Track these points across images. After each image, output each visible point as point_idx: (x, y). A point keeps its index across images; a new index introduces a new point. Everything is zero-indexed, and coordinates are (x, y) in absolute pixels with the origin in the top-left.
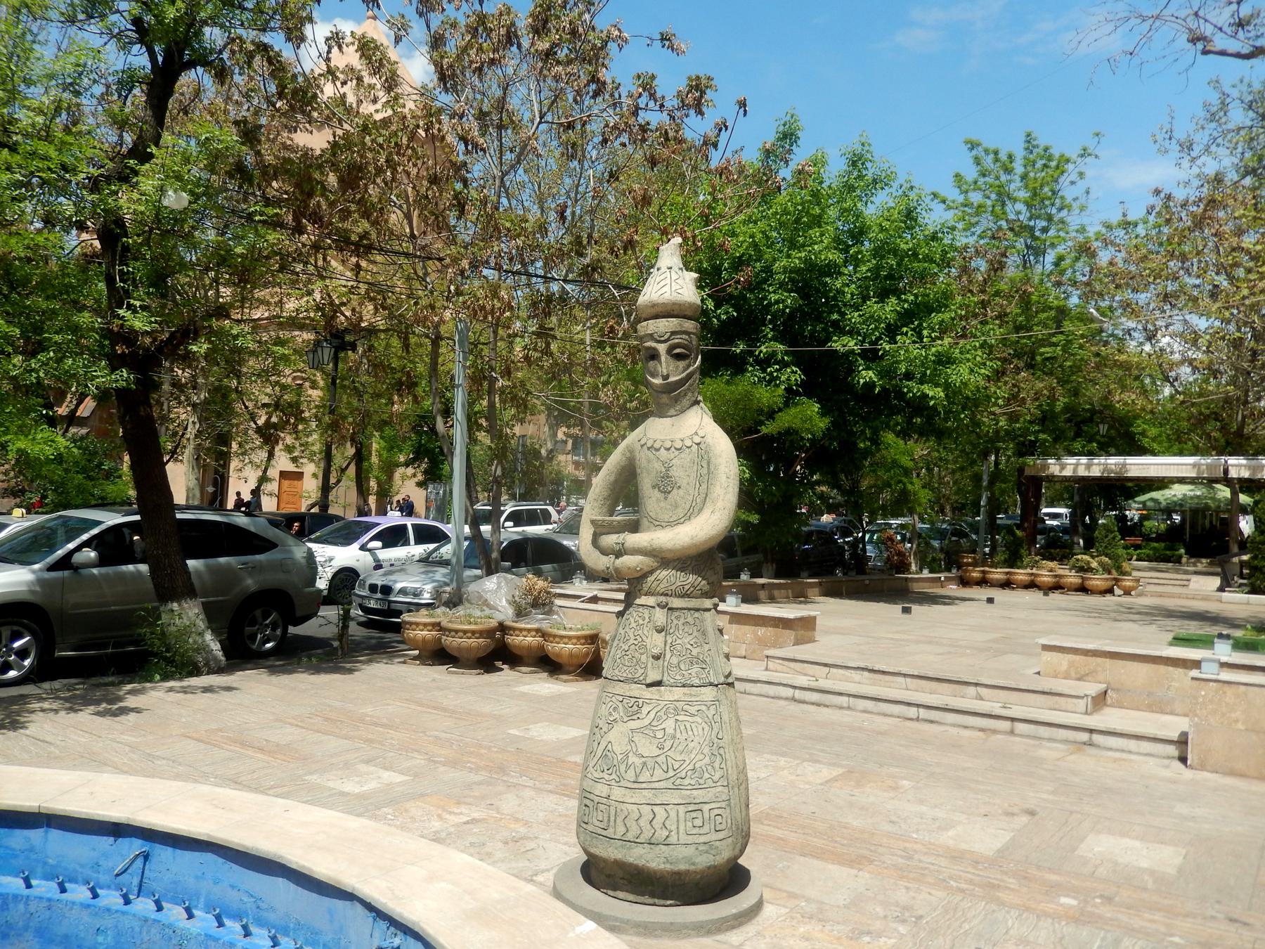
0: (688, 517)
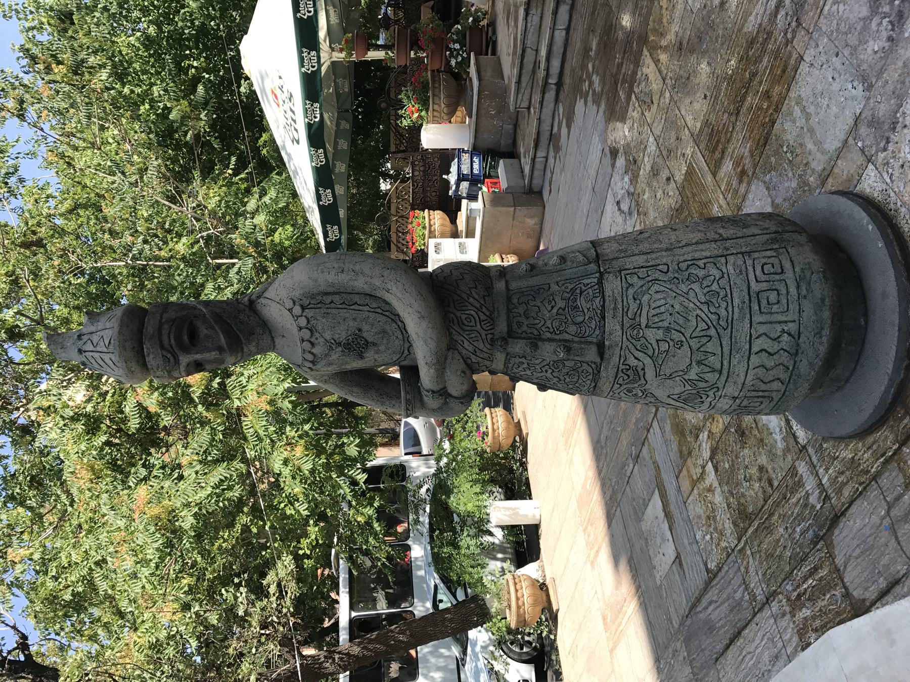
0: (396, 318)
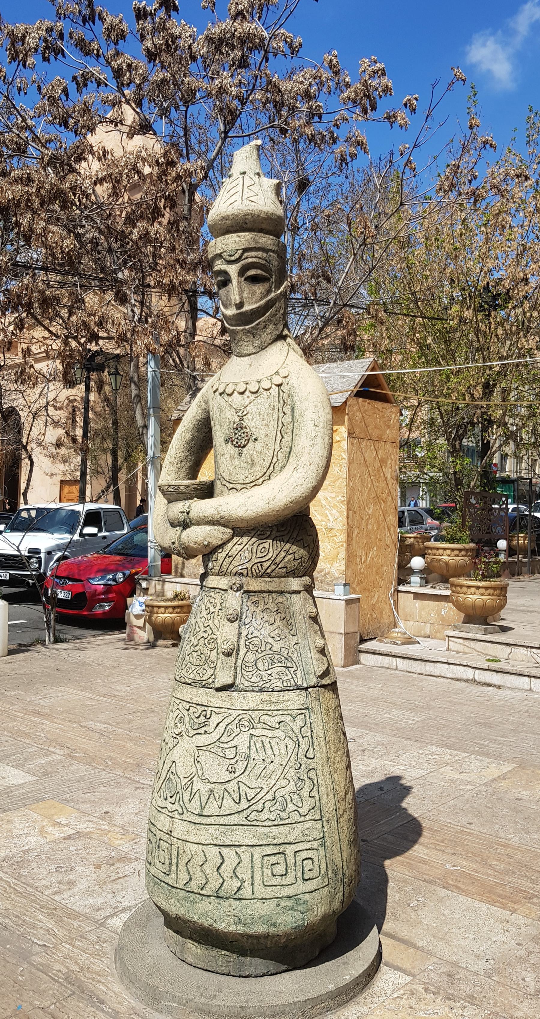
0: (267, 476)
